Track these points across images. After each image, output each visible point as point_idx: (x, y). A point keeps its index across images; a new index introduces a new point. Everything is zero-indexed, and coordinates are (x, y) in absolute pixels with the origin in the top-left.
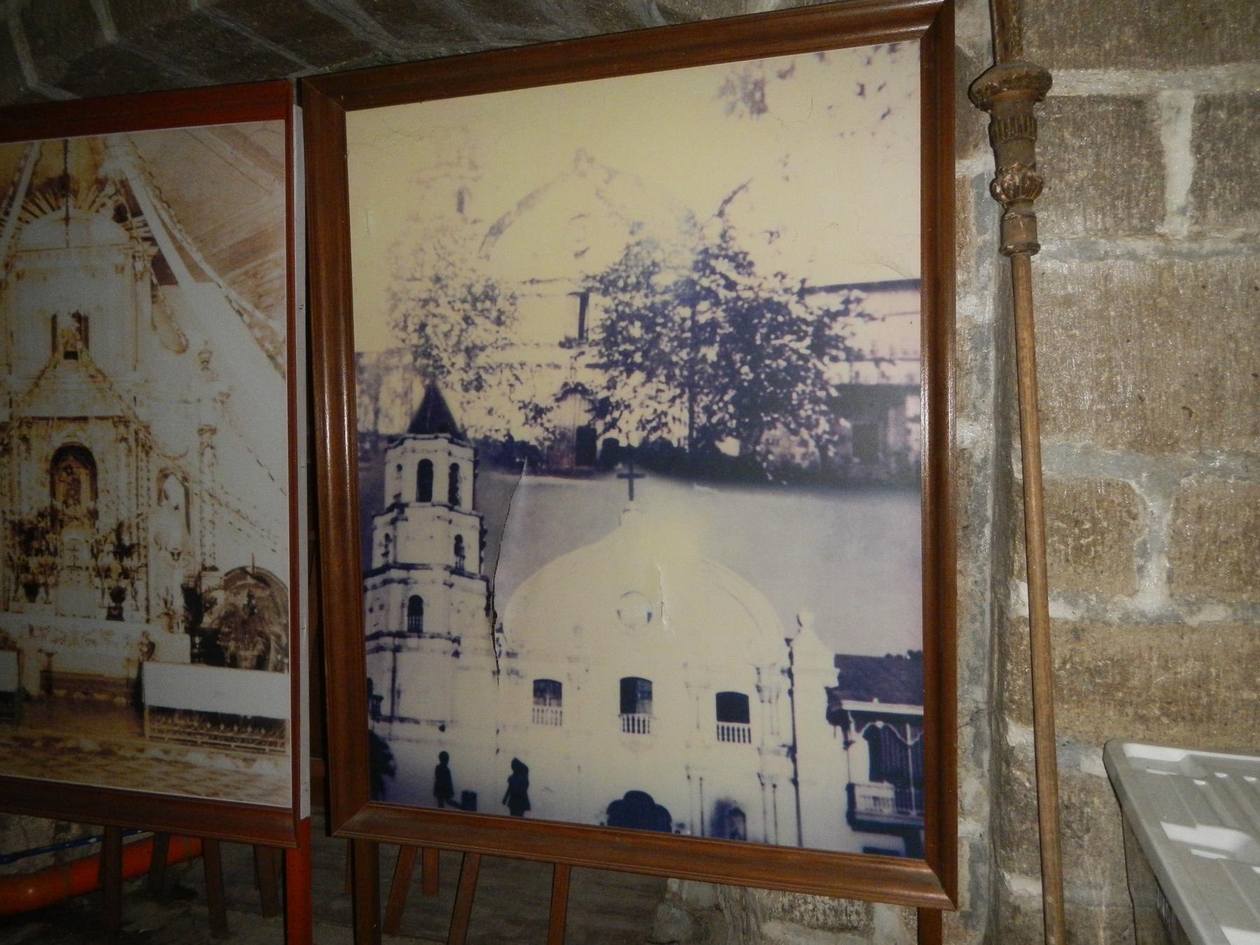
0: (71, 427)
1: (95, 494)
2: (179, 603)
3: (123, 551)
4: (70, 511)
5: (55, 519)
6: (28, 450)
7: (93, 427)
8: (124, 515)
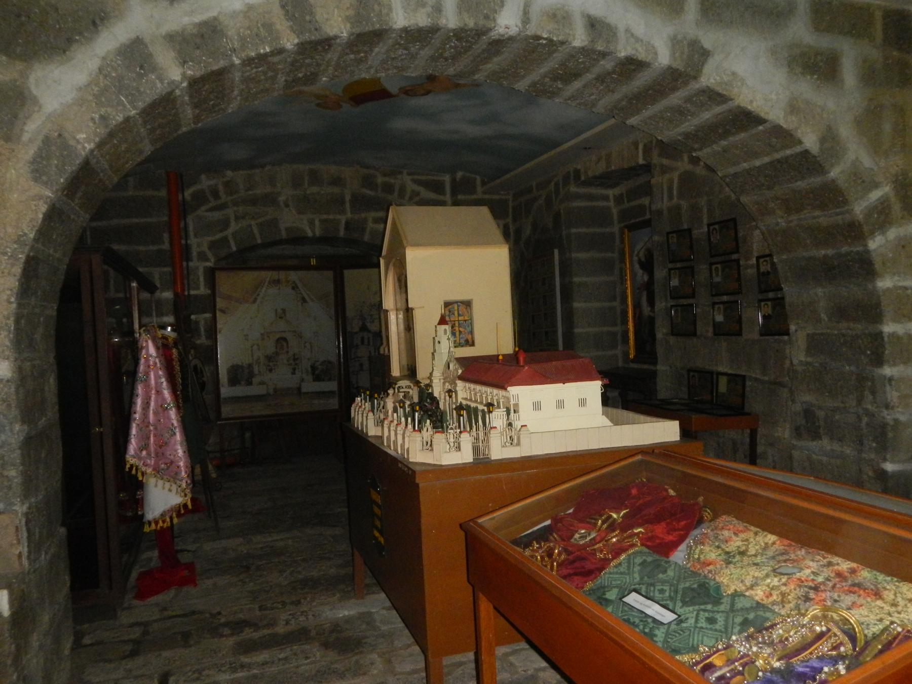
2: (310, 369)
3: (295, 359)
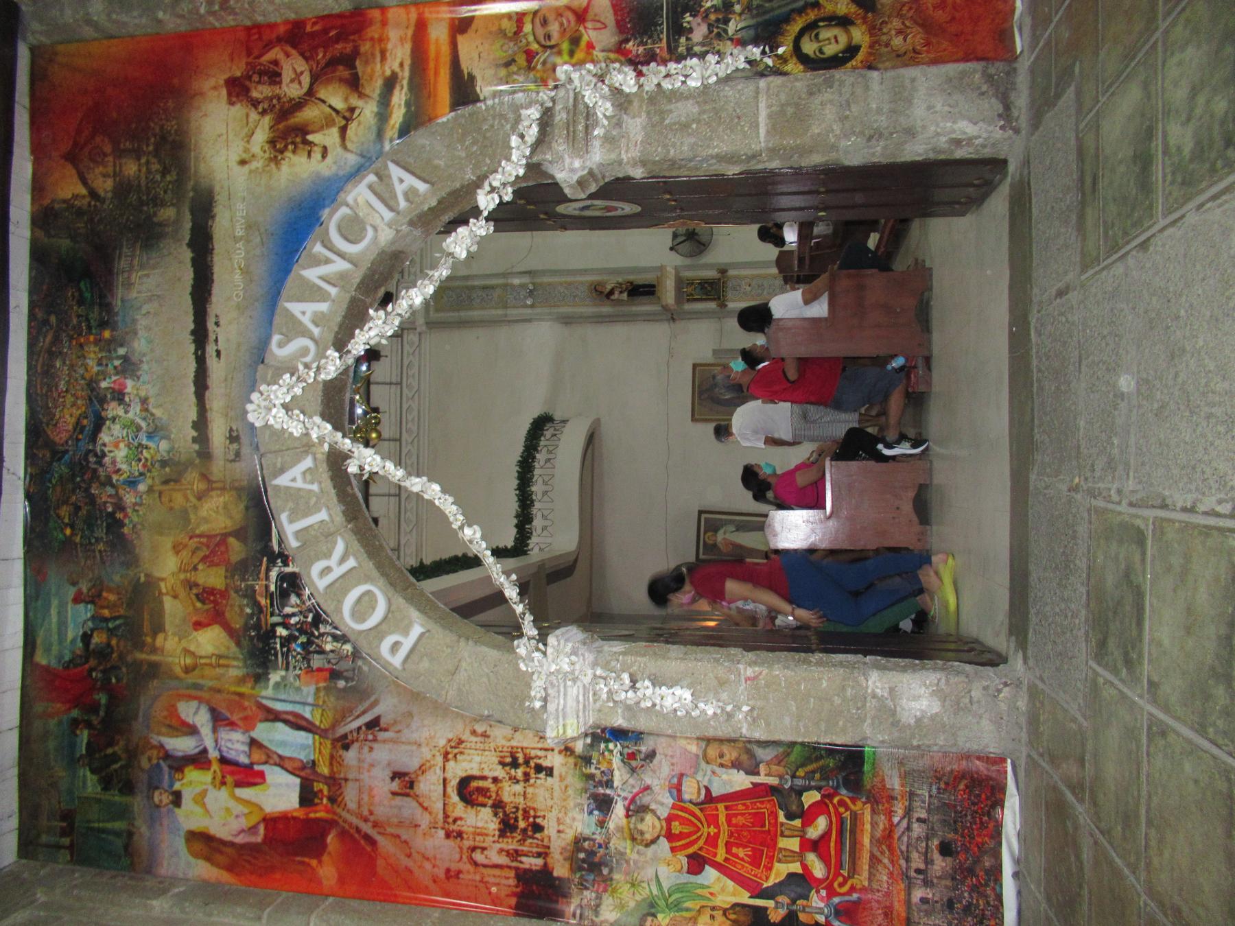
0: (449, 790)
1: (484, 778)
3: (515, 764)
4: (494, 795)
5: (498, 805)
6: (461, 819)
7: (449, 775)
8: (496, 760)
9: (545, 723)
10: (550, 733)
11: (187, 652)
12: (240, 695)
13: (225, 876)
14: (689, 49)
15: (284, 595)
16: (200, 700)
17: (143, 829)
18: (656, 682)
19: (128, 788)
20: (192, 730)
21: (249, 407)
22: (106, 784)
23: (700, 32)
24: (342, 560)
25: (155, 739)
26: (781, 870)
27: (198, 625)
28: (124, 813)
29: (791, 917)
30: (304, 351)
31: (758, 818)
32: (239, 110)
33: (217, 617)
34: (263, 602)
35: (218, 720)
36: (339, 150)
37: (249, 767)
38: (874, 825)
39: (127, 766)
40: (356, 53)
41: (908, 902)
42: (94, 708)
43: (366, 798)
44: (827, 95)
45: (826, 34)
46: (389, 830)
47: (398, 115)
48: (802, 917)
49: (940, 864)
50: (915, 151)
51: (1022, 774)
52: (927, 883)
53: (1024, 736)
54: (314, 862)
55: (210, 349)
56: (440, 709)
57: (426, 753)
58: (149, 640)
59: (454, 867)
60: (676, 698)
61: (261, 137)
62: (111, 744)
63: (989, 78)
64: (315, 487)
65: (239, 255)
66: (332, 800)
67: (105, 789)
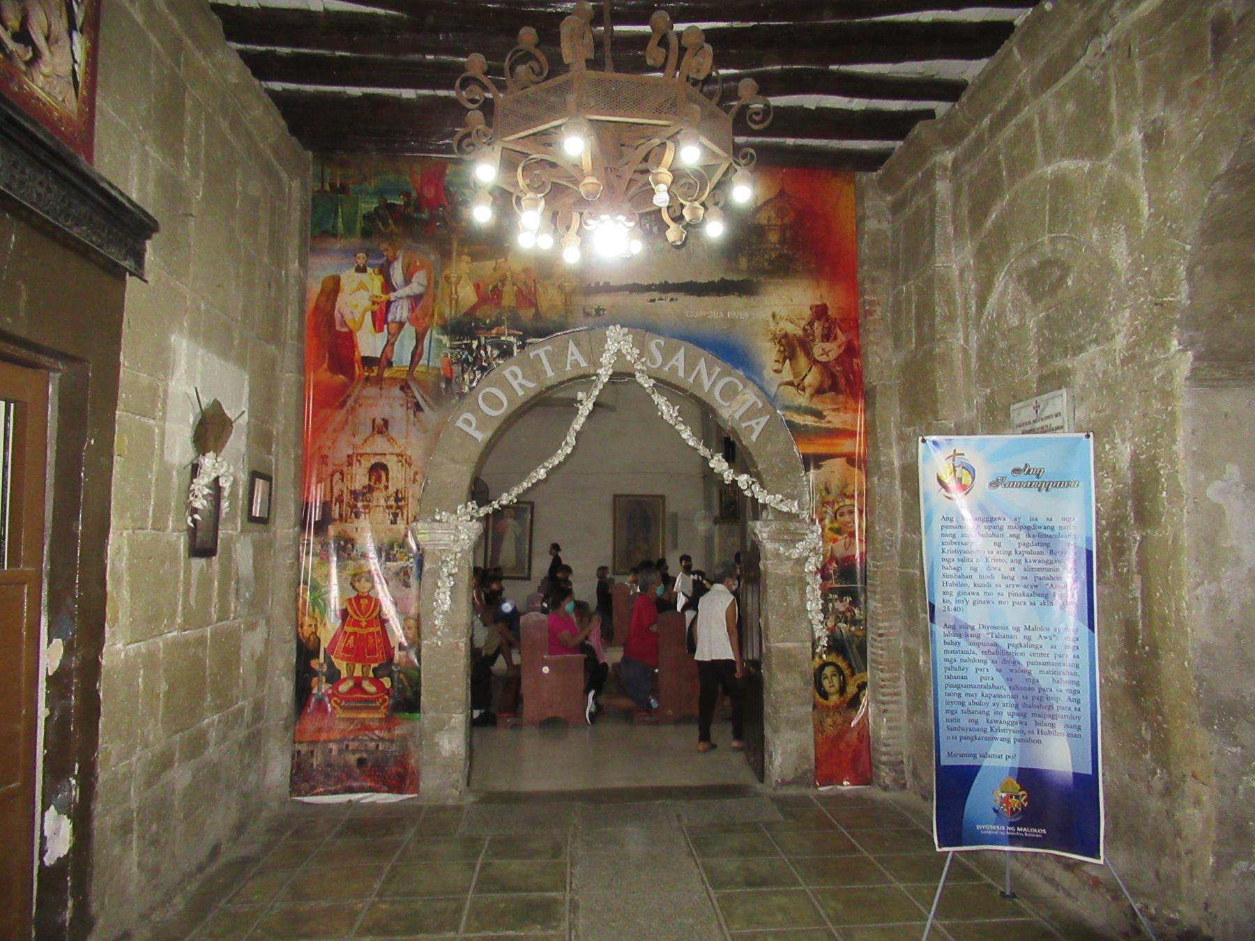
1: (387, 480)
3: (397, 500)
5: (370, 489)
7: (388, 457)
9: (425, 521)
10: (419, 525)
11: (459, 278)
12: (433, 315)
13: (310, 306)
14: (831, 600)
15: (498, 346)
16: (428, 287)
17: (339, 244)
18: (452, 589)
19: (366, 234)
20: (407, 281)
21: (618, 327)
22: (368, 218)
23: (840, 606)
24: (521, 385)
25: (400, 254)
26: (341, 666)
27: (477, 287)
28: (349, 230)
29: (314, 673)
30: (653, 361)
31: (373, 652)
32: (807, 313)
33: (483, 300)
34: (494, 332)
35: (416, 299)
36: (779, 381)
37: (386, 322)
38: (373, 719)
39: (382, 234)
40: (838, 392)
41: (330, 741)
42: (418, 209)
43: (371, 401)
44: (800, 683)
45: (836, 680)
46: (350, 418)
47: (799, 419)
48: (315, 679)
49: (353, 759)
50: (768, 732)
51: (411, 803)
52: (340, 751)
53: (432, 803)
54: (325, 366)
55: (656, 295)
56: (429, 451)
57: (402, 442)
58: (466, 250)
59: (330, 461)
60: (444, 600)
61: (790, 329)
62: (395, 222)
63: (805, 773)
64: (568, 367)
65: (716, 315)
66: (367, 379)
67: (364, 217)
